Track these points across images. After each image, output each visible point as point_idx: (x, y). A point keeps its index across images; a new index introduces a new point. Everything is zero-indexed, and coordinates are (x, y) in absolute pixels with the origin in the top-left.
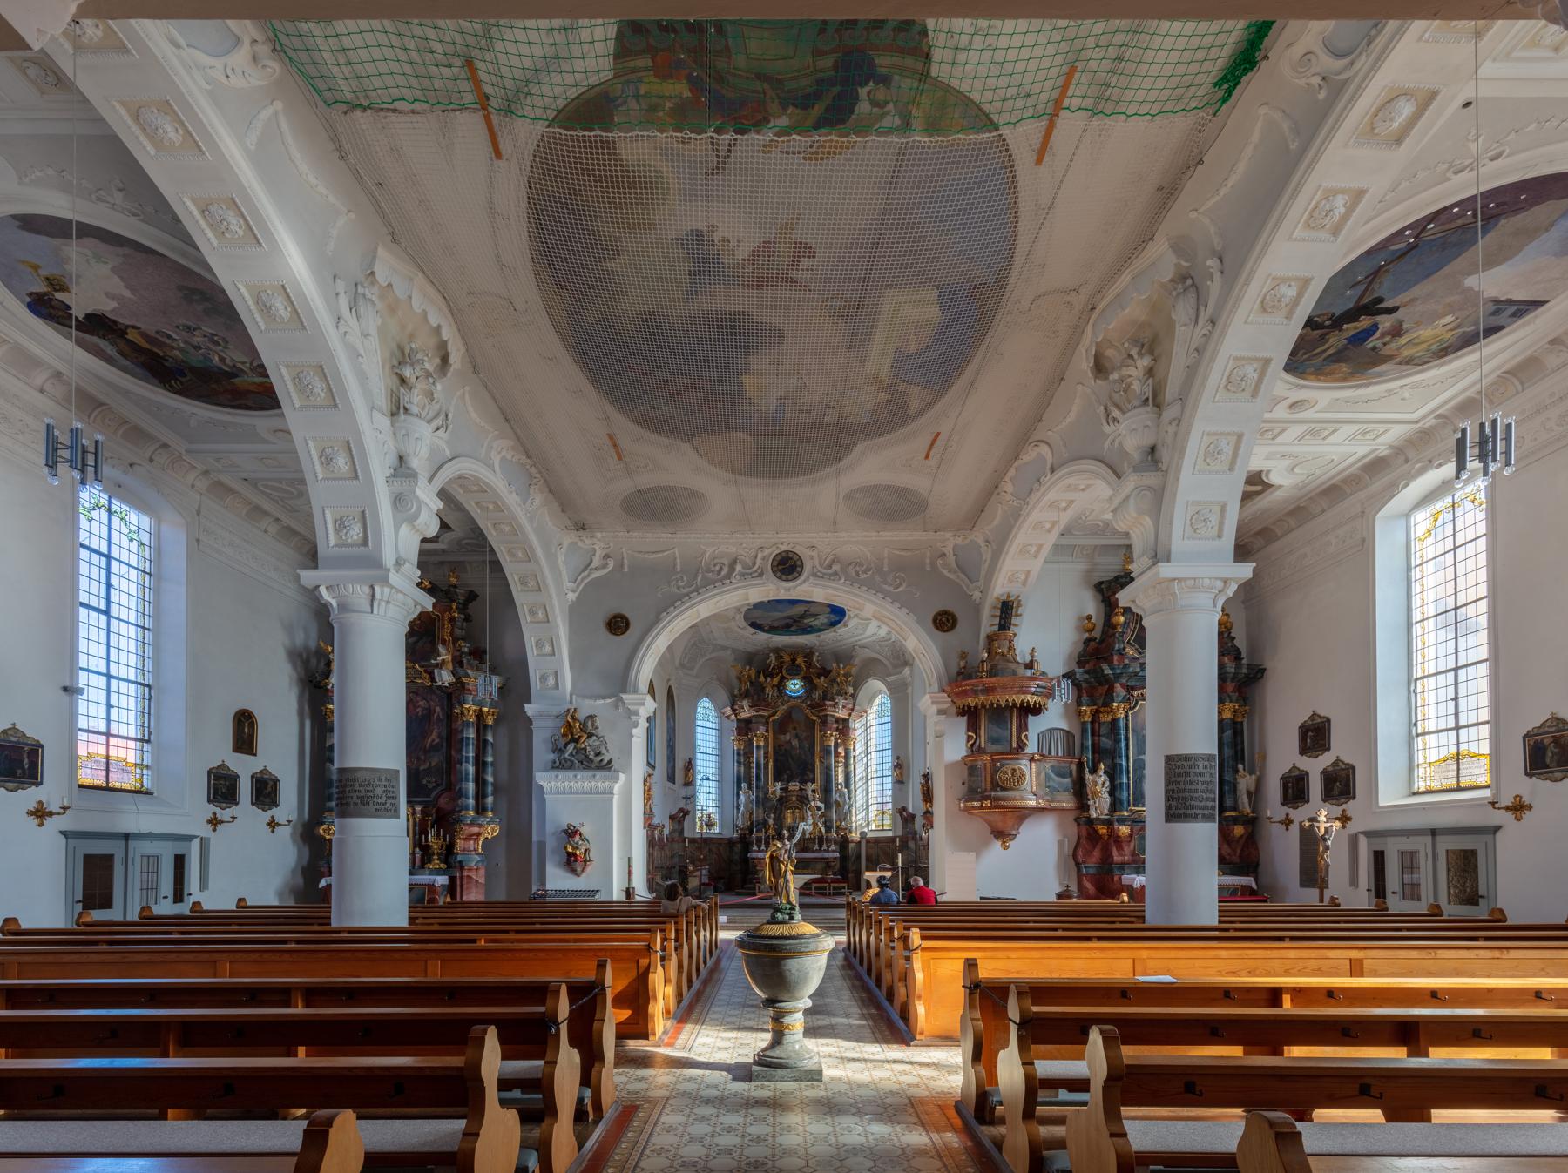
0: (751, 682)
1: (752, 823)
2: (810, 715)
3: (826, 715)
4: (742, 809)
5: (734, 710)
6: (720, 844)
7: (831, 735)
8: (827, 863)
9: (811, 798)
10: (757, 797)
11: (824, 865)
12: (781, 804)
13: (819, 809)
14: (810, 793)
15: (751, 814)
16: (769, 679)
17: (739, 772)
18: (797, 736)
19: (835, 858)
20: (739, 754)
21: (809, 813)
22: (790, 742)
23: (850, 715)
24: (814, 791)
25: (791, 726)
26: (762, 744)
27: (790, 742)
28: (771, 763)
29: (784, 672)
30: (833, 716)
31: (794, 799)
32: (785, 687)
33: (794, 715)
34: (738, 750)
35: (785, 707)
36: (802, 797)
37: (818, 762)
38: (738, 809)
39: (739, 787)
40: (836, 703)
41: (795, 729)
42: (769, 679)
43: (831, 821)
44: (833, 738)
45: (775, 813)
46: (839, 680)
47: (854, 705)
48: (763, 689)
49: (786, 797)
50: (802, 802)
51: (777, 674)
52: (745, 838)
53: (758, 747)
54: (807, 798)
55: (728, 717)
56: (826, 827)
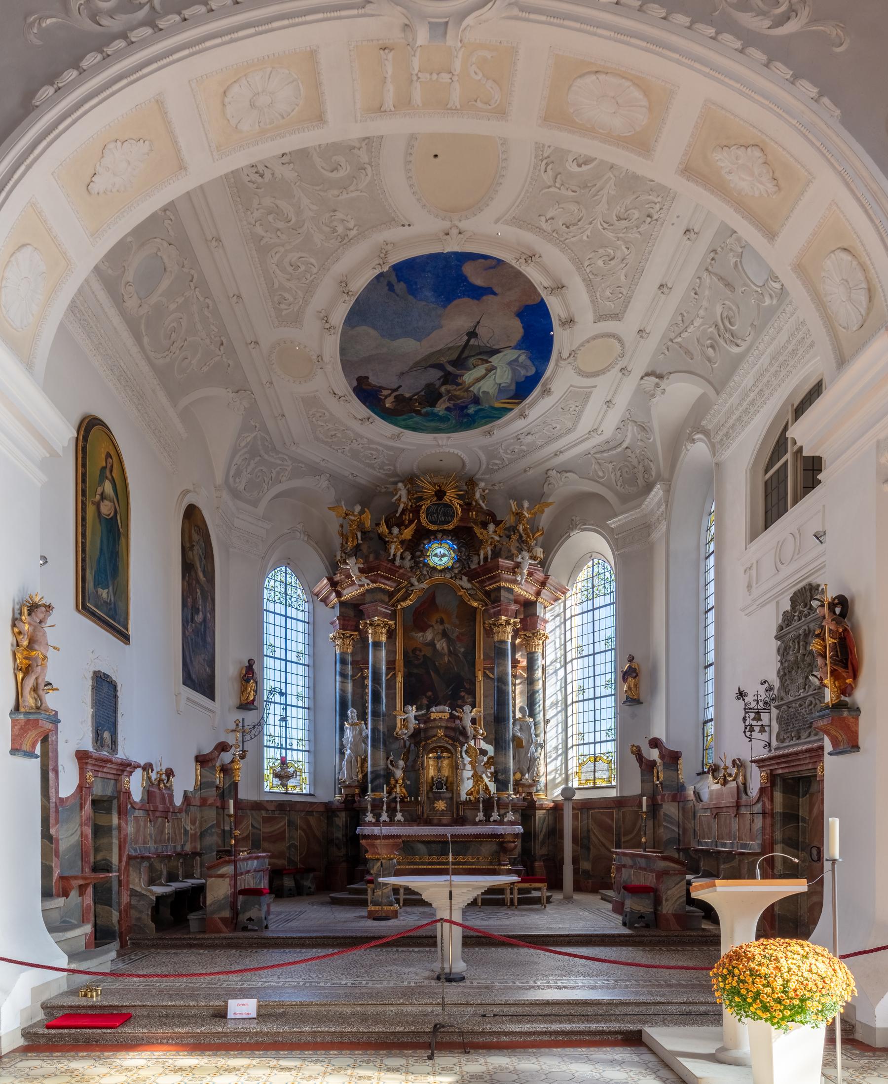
4: (348, 752)
9: (470, 731)
10: (374, 730)
11: (494, 847)
14: (468, 724)
15: (364, 760)
19: (516, 835)
21: (467, 759)
24: (474, 721)
29: (423, 516)
31: (441, 733)
36: (454, 729)
38: (342, 753)
39: (343, 716)
43: (506, 771)
45: (406, 760)
49: (426, 730)
50: (455, 740)
52: (354, 801)
54: (463, 732)
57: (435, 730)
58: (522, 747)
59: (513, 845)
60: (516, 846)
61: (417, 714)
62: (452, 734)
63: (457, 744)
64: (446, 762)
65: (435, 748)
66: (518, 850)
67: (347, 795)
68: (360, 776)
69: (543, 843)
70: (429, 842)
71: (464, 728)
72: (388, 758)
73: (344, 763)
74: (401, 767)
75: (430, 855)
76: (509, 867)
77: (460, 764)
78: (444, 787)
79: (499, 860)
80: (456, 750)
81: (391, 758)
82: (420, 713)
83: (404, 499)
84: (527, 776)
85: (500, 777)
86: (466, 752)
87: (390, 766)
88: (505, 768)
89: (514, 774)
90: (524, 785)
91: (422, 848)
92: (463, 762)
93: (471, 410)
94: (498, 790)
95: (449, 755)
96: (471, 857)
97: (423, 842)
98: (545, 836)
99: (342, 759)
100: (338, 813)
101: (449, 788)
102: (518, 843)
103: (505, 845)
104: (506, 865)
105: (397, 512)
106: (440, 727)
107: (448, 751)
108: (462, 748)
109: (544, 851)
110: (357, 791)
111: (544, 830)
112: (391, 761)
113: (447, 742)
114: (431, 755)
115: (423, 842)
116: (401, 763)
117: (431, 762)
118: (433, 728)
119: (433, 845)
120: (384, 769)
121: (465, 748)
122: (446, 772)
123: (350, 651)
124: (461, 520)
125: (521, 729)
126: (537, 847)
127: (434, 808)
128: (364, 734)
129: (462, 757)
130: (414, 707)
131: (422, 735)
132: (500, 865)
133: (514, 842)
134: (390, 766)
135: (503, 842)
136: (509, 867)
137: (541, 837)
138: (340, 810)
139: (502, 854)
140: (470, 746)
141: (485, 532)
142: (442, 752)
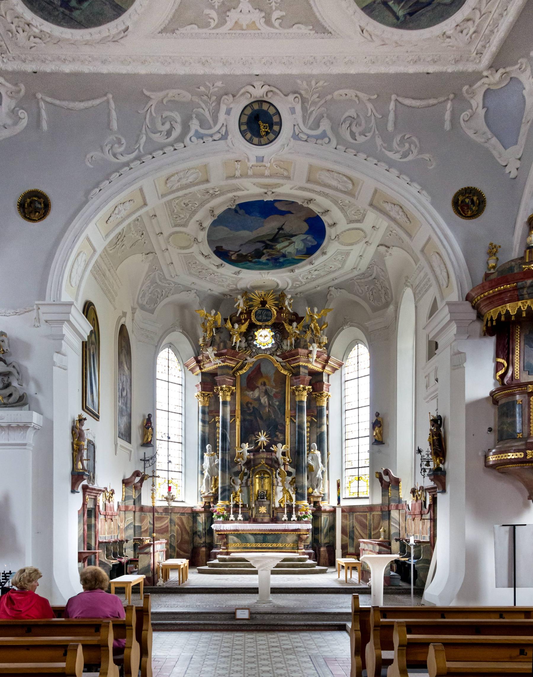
0: (217, 329)
1: (217, 490)
2: (280, 368)
3: (299, 367)
4: (206, 474)
5: (198, 362)
6: (183, 514)
7: (304, 389)
8: (299, 536)
9: (281, 461)
10: (223, 460)
11: (295, 538)
12: (249, 469)
13: (289, 474)
14: (279, 456)
15: (216, 480)
16: (236, 326)
17: (203, 432)
18: (266, 393)
19: (308, 530)
20: (203, 412)
21: (279, 479)
22: (258, 399)
23: (324, 368)
24: (284, 454)
25: (261, 381)
26: (228, 399)
27: (258, 399)
28: (238, 423)
30: (306, 367)
31: (263, 462)
32: (254, 338)
33: (263, 369)
34: (204, 407)
35: (254, 360)
36: (271, 459)
37: (288, 420)
38: (203, 474)
39: (203, 450)
40: (311, 352)
41: (264, 384)
42: (236, 326)
43: (302, 487)
44: (305, 393)
45: (242, 479)
46: (312, 325)
47: (329, 357)
48: (231, 336)
49: (254, 460)
50: (271, 466)
51: (246, 320)
53: (225, 403)
54: (277, 461)
55: (192, 370)
56: (297, 493)
57: (260, 460)
58: (313, 471)
59: (306, 536)
60: (307, 537)
61: (249, 449)
62: (270, 463)
63: (273, 469)
64: (267, 480)
65: (259, 472)
66: (310, 540)
67: (205, 502)
68: (214, 489)
69: (326, 535)
70: (256, 534)
71: (277, 459)
72: (231, 478)
73: (204, 481)
74: (239, 484)
75: (256, 542)
76: (304, 550)
77: (275, 482)
78: (265, 498)
79: (298, 546)
80: (272, 473)
81: (233, 478)
82: (251, 448)
83: (242, 305)
84: (316, 490)
85: (300, 491)
86: (279, 474)
87: (232, 483)
88: (302, 485)
89: (308, 489)
90: (314, 496)
91: (252, 538)
92: (277, 481)
93: (281, 260)
94: (297, 499)
95: (268, 476)
96: (281, 544)
97: (252, 534)
98: (327, 530)
99: (203, 478)
100: (200, 514)
101: (268, 498)
102: (310, 535)
103: (301, 536)
104: (302, 549)
105: (237, 313)
106: (263, 458)
107: (268, 473)
108: (276, 471)
109: (327, 541)
110: (212, 500)
111: (327, 526)
112: (233, 480)
113: (267, 468)
114: (257, 476)
115: (252, 534)
116: (239, 481)
117: (257, 480)
118: (259, 458)
119: (259, 536)
120: (229, 486)
121: (278, 471)
122: (267, 487)
123: (207, 405)
124: (277, 318)
125: (312, 459)
126: (323, 538)
127: (259, 511)
128: (216, 463)
129: (276, 477)
130: (247, 444)
131: (252, 463)
132: (298, 549)
133: (307, 534)
134: (232, 483)
135: (300, 535)
136: (304, 550)
137: (325, 531)
138: (201, 512)
139: (299, 542)
140: (281, 470)
141: (291, 327)
142: (264, 474)
